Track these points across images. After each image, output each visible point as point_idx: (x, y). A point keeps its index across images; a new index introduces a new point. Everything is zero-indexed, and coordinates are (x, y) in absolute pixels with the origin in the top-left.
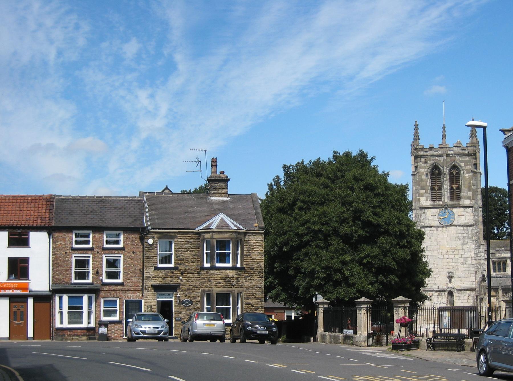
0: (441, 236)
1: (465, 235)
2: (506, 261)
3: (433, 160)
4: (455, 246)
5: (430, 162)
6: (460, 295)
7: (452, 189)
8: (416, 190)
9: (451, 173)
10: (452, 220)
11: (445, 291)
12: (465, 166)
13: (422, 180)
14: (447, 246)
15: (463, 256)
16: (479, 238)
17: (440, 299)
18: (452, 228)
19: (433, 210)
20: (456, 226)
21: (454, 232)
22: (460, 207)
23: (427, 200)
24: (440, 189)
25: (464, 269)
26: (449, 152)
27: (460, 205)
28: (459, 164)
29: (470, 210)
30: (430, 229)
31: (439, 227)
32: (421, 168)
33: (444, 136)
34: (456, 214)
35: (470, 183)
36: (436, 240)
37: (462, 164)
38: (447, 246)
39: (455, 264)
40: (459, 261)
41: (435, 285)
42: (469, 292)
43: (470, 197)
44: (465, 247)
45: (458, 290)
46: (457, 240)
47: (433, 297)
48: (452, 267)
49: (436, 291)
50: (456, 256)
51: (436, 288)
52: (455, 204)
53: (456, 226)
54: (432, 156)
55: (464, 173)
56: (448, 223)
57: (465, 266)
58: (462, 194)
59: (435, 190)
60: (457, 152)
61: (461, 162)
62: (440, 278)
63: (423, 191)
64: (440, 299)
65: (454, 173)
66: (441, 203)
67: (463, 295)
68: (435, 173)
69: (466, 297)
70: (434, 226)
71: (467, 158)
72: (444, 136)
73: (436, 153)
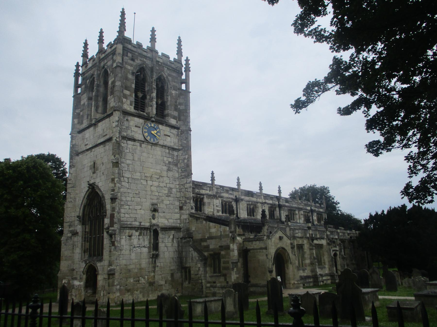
0: (145, 154)
1: (170, 160)
2: (203, 198)
4: (159, 171)
14: (152, 170)
15: (168, 185)
17: (141, 240)
19: (136, 119)
20: (162, 146)
21: (159, 153)
28: (167, 77)
29: (175, 131)
31: (143, 142)
35: (176, 102)
36: (139, 159)
37: (170, 78)
39: (160, 194)
41: (135, 220)
42: (173, 232)
43: (176, 117)
44: (170, 174)
46: (162, 164)
47: (133, 237)
48: (155, 198)
49: (137, 229)
50: (161, 185)
51: (137, 224)
55: (171, 88)
57: (170, 198)
58: (166, 112)
62: (142, 212)
63: (127, 92)
64: (141, 240)
69: (170, 240)
70: (138, 140)
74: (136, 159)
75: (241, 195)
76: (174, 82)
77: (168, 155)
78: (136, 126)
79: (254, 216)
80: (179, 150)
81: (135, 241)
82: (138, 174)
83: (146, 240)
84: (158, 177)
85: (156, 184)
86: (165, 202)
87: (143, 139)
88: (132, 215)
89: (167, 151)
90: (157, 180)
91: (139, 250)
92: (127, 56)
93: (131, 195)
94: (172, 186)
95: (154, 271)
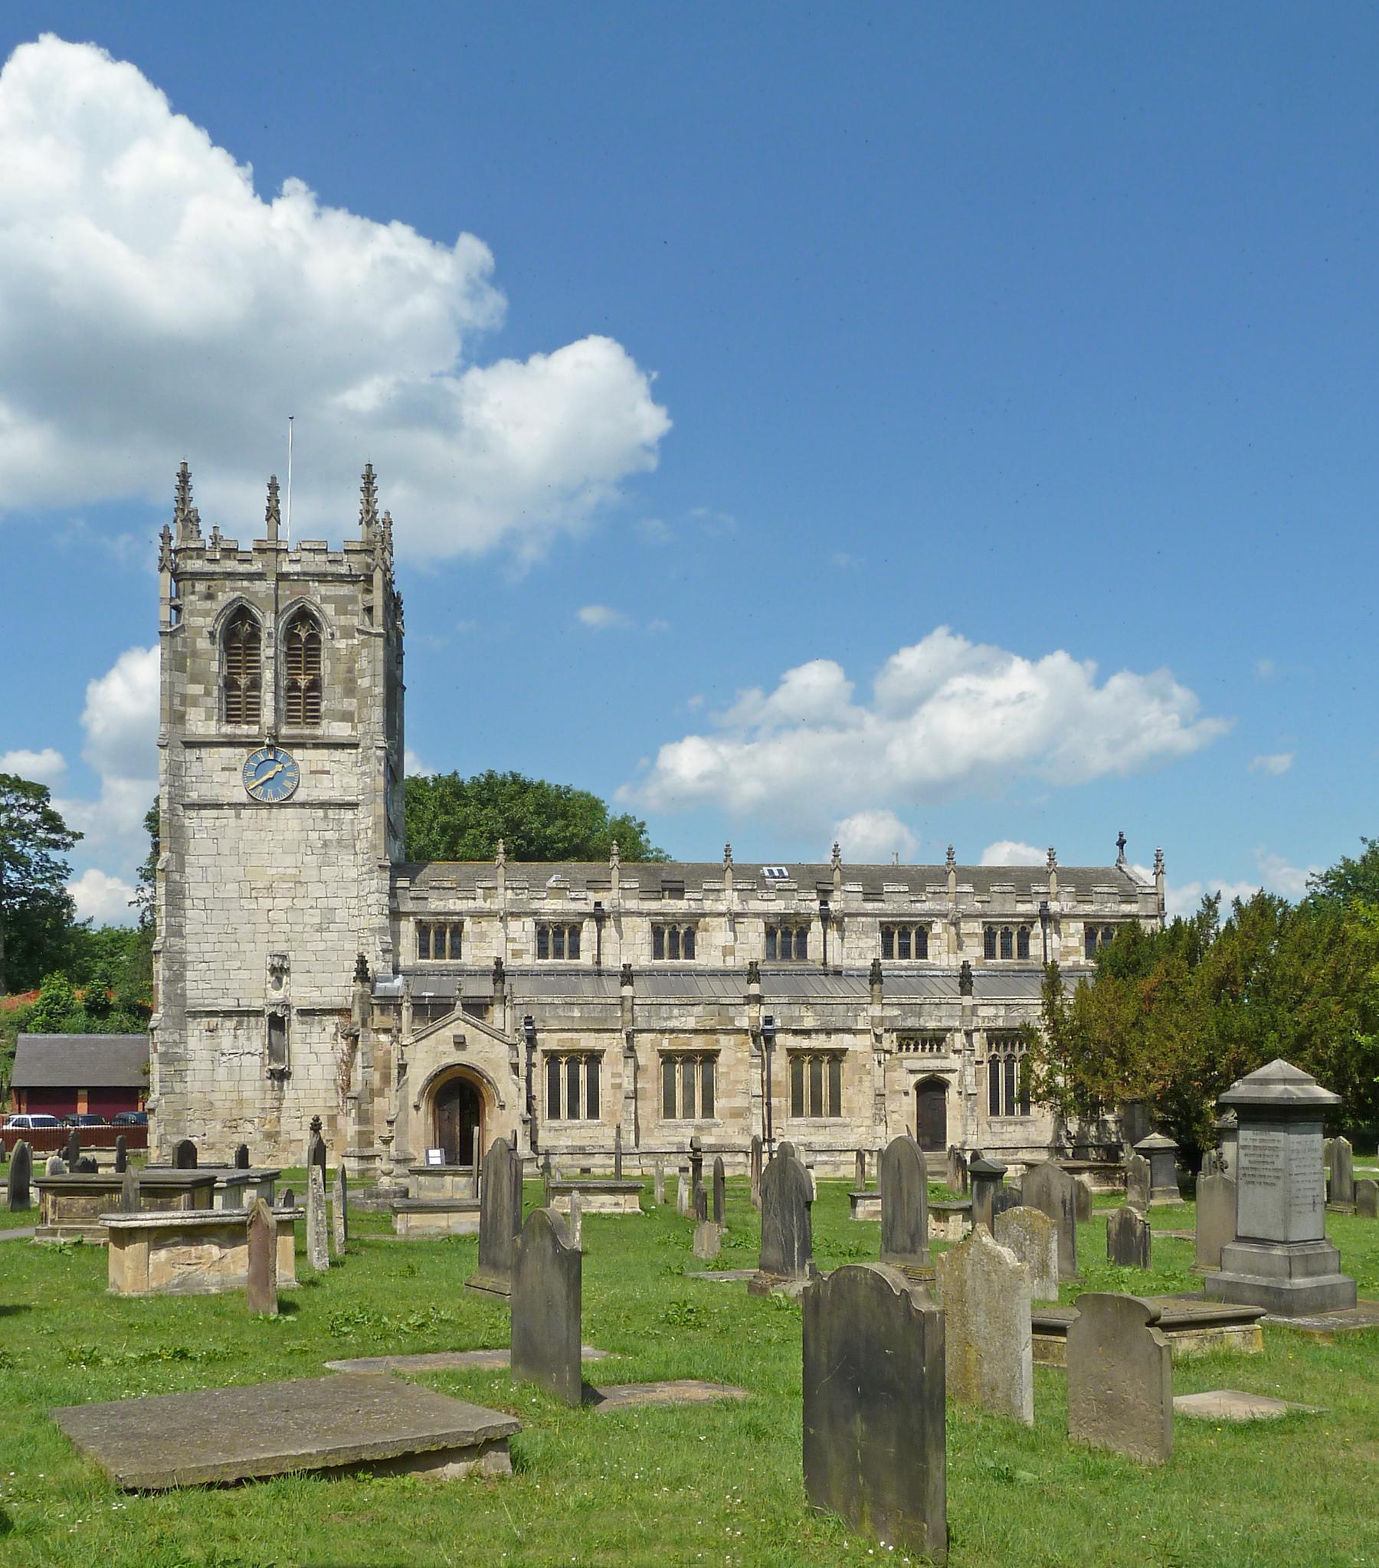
0: (248, 835)
1: (328, 835)
2: (462, 923)
3: (233, 590)
4: (294, 871)
5: (224, 598)
6: (306, 1028)
7: (293, 686)
8: (172, 683)
9: (290, 636)
10: (288, 784)
11: (258, 1014)
13: (195, 654)
15: (322, 903)
16: (374, 847)
17: (242, 1040)
19: (223, 750)
20: (303, 805)
21: (295, 824)
22: (316, 746)
23: (208, 718)
24: (255, 685)
25: (322, 946)
26: (286, 568)
27: (317, 737)
28: (320, 611)
30: (214, 813)
31: (243, 805)
32: (192, 614)
33: (273, 514)
34: (303, 768)
35: (350, 670)
36: (235, 851)
37: (329, 609)
38: (273, 871)
39: (298, 928)
40: (307, 919)
42: (336, 1019)
44: (328, 873)
45: (303, 1013)
47: (220, 1033)
48: (283, 937)
49: (228, 1014)
51: (228, 1004)
52: (302, 736)
53: (303, 805)
54: (229, 576)
56: (276, 794)
59: (239, 688)
60: (312, 569)
61: (325, 599)
63: (197, 689)
65: (303, 635)
66: (254, 729)
67: (317, 1029)
68: (238, 631)
69: (326, 1037)
70: (229, 804)
71: (345, 590)
72: (273, 514)
73: (243, 568)
76: (345, 614)
78: (223, 769)
79: (690, 954)
80: (353, 805)
81: (226, 1041)
83: (253, 1039)
84: (292, 885)
87: (245, 799)
88: (214, 984)
91: (236, 1060)
92: (193, 593)
93: (212, 938)
94: (333, 903)
95: (279, 1109)
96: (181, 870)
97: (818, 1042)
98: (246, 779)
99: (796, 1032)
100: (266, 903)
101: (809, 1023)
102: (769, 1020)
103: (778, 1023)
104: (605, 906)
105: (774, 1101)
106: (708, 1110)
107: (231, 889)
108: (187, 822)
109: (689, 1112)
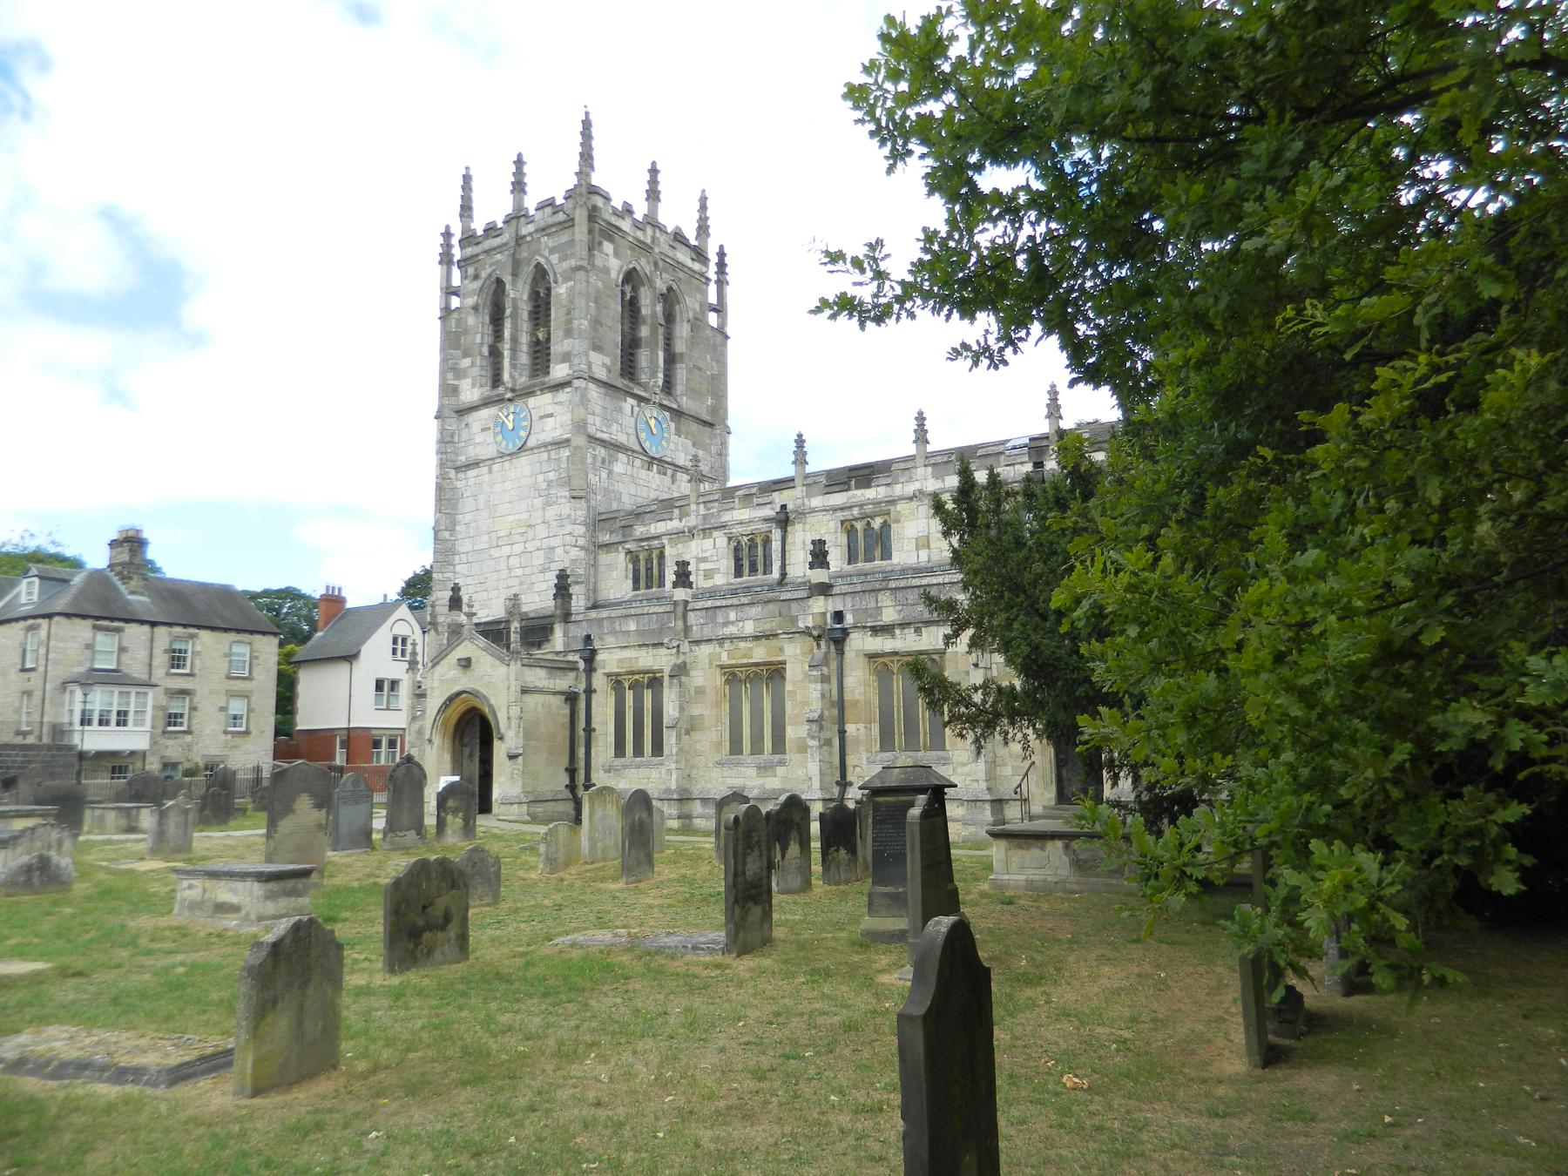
0: (497, 488)
1: (552, 476)
4: (525, 516)
12: (562, 259)
14: (511, 518)
15: (546, 544)
18: (524, 461)
23: (473, 386)
29: (563, 395)
39: (528, 571)
44: (551, 513)
48: (516, 582)
50: (530, 546)
61: (552, 251)
63: (466, 362)
74: (482, 506)
75: (809, 495)
77: (545, 467)
79: (886, 554)
82: (485, 538)
85: (518, 548)
86: (537, 587)
89: (545, 455)
90: (519, 538)
96: (452, 528)
97: (906, 642)
98: (495, 435)
99: (877, 630)
100: (506, 550)
101: (889, 615)
102: (839, 616)
103: (849, 619)
104: (790, 507)
105: (850, 728)
106: (779, 744)
107: (483, 541)
108: (459, 484)
109: (757, 749)
